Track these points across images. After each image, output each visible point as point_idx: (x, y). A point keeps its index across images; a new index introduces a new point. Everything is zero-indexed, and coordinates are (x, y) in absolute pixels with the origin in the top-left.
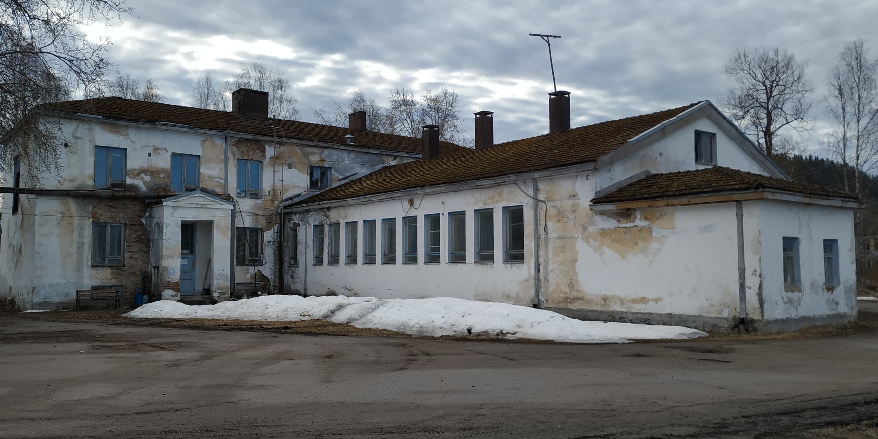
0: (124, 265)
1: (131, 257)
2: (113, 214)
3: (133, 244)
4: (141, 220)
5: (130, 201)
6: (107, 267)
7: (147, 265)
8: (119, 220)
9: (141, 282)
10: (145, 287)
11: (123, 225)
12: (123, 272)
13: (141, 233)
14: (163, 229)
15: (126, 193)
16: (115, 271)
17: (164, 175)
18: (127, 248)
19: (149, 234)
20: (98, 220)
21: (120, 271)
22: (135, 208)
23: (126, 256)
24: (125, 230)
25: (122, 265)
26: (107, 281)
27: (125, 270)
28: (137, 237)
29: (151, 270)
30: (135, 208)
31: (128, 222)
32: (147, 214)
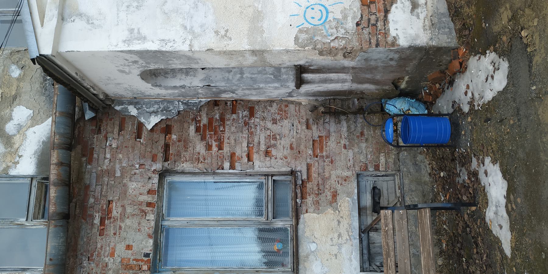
0: (293, 173)
1: (267, 153)
2: (129, 210)
3: (226, 149)
4: (149, 127)
5: (90, 161)
6: (297, 224)
7: (292, 107)
8: (150, 192)
9: (344, 124)
10: (360, 111)
11: (169, 179)
12: (314, 175)
13: (192, 128)
14: (147, 52)
15: (53, 177)
16: (310, 200)
17: (14, 67)
18: (237, 165)
19: (195, 104)
20: (147, 255)
21: (309, 185)
22: (114, 146)
23: (265, 170)
24: (183, 173)
25: (289, 178)
26: (345, 223)
27: (308, 169)
28: (203, 138)
29: (307, 94)
30: (114, 146)
31: (158, 166)
32: (133, 111)
